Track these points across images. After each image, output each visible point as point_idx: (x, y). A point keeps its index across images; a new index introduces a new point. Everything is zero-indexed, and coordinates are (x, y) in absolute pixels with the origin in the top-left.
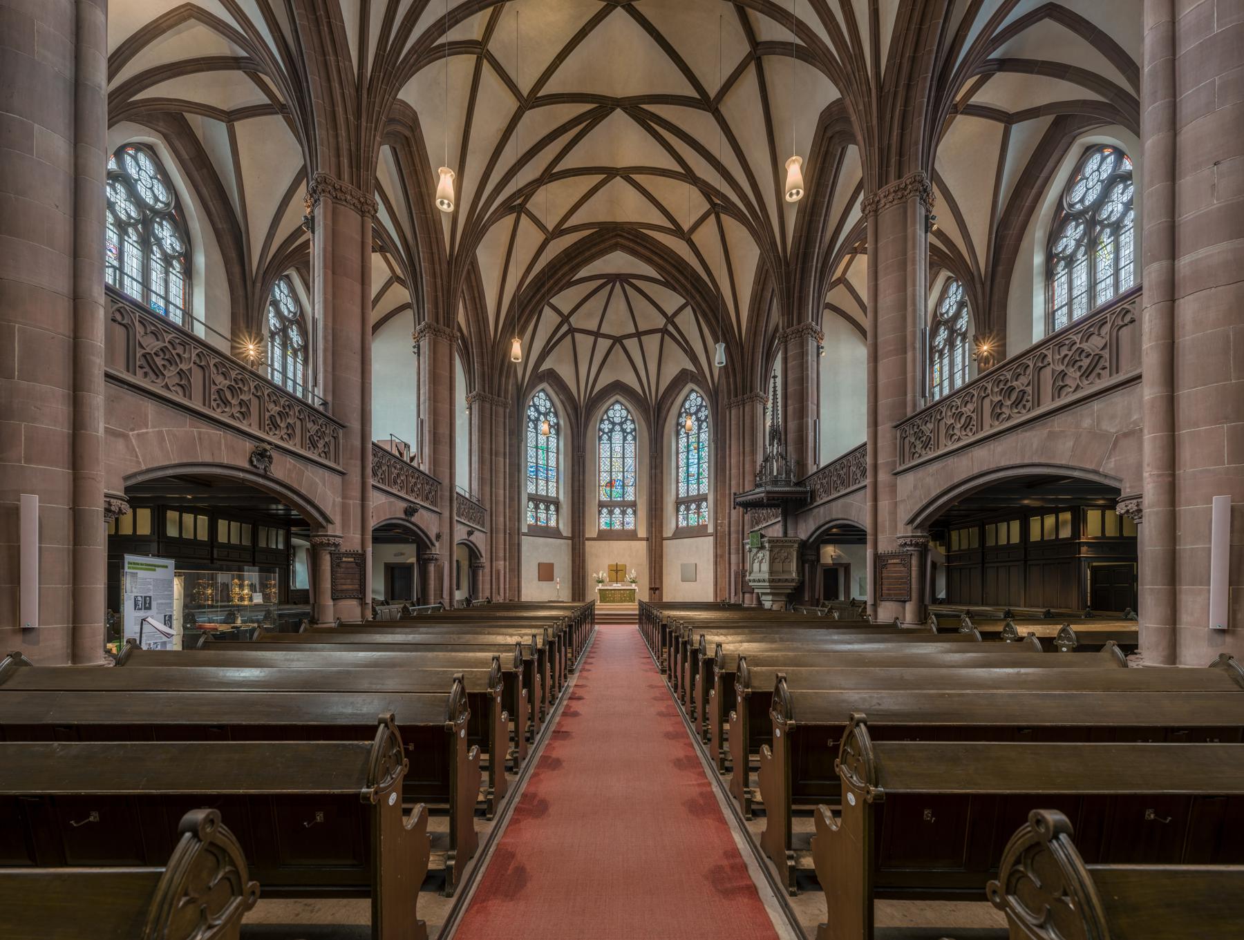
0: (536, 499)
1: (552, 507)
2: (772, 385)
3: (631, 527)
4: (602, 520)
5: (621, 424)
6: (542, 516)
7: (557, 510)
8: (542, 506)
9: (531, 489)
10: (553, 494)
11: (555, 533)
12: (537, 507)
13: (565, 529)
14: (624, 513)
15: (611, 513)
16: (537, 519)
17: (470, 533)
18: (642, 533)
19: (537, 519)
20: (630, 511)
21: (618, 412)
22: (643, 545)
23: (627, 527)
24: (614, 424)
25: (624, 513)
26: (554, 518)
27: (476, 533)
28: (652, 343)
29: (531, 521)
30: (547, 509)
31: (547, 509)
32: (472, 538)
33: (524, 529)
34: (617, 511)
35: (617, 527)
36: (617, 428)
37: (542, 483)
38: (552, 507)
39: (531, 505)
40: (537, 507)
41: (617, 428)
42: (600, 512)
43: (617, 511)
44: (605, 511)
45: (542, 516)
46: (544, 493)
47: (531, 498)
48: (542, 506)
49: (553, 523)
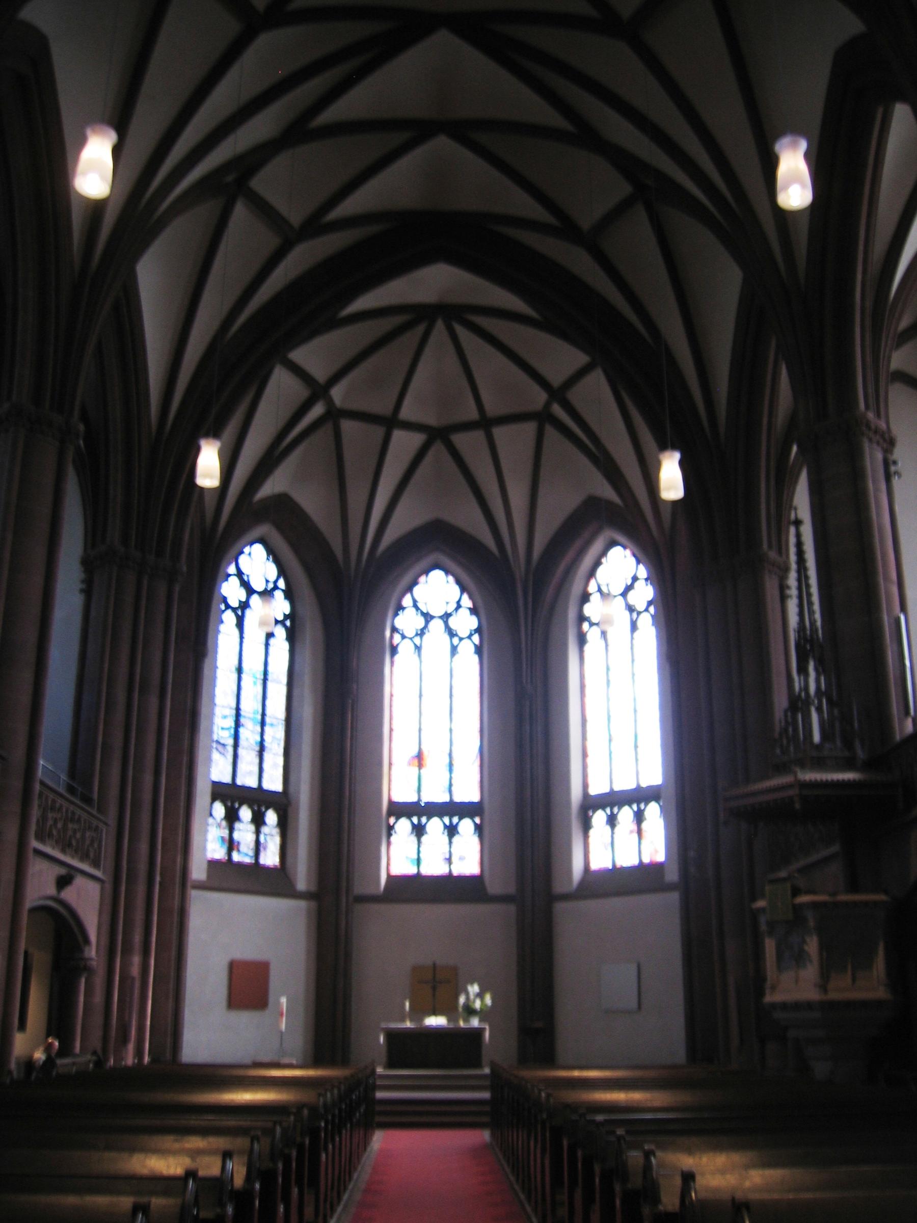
0: (231, 796)
1: (271, 817)
2: (792, 540)
5: (446, 617)
7: (283, 825)
8: (246, 813)
9: (219, 769)
10: (274, 782)
12: (232, 817)
16: (232, 845)
17: (63, 882)
19: (232, 845)
21: (437, 589)
24: (428, 617)
27: (79, 881)
28: (515, 441)
29: (215, 850)
30: (258, 821)
31: (258, 821)
32: (68, 894)
33: (198, 872)
36: (437, 626)
37: (248, 759)
38: (271, 817)
39: (219, 810)
40: (232, 817)
41: (437, 626)
46: (252, 783)
48: (246, 813)
49: (271, 858)
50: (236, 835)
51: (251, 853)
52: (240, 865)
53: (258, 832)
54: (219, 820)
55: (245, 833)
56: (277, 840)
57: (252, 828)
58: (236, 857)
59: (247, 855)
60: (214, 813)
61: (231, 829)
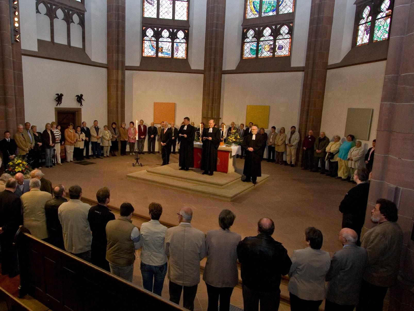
0: (158, 25)
1: (181, 34)
3: (285, 52)
4: (247, 47)
6: (166, 45)
7: (187, 37)
8: (165, 33)
11: (181, 66)
12: (157, 35)
13: (197, 63)
14: (276, 34)
15: (259, 35)
16: (158, 49)
18: (299, 60)
19: (158, 49)
23: (279, 53)
25: (276, 34)
26: (182, 47)
30: (173, 36)
31: (173, 36)
34: (267, 31)
35: (266, 53)
38: (181, 34)
40: (157, 35)
44: (251, 33)
45: (166, 45)
46: (170, 17)
47: (147, 23)
48: (165, 33)
49: (181, 54)
50: (160, 44)
51: (170, 53)
52: (163, 58)
53: (173, 43)
54: (150, 37)
56: (184, 46)
57: (64, 24)
58: (160, 55)
60: (147, 34)
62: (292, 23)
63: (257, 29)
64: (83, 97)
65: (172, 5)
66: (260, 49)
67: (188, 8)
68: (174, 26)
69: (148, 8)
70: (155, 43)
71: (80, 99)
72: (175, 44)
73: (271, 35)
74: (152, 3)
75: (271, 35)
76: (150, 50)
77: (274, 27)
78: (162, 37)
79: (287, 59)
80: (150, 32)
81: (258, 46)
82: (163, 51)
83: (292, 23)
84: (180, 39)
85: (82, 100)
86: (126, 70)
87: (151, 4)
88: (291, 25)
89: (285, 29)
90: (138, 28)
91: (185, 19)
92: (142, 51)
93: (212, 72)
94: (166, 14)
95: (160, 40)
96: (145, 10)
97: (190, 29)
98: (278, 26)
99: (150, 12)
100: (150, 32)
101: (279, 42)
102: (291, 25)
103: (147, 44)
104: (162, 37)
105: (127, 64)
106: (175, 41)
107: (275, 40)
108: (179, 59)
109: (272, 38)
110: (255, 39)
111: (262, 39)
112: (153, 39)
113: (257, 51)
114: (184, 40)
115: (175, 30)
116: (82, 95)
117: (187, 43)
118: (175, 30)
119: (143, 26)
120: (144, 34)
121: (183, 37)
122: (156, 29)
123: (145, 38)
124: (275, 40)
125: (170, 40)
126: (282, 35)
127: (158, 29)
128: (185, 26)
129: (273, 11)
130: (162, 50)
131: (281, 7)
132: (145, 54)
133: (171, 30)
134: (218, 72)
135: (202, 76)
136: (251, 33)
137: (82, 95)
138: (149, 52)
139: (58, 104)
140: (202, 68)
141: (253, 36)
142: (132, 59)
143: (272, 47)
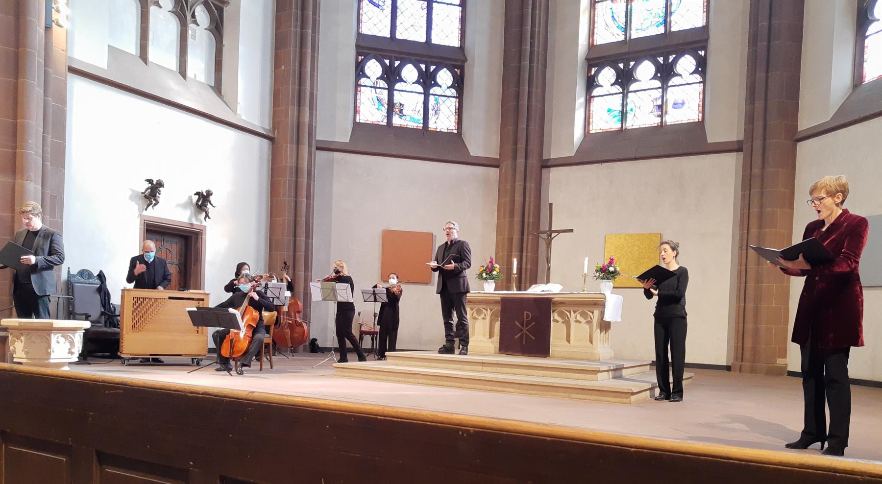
0: (391, 53)
1: (445, 77)
7: (459, 84)
8: (410, 72)
10: (446, 34)
11: (446, 148)
12: (391, 76)
13: (482, 140)
14: (665, 73)
15: (625, 79)
18: (727, 127)
20: (686, 64)
22: (729, 165)
25: (665, 73)
30: (427, 81)
31: (427, 81)
34: (645, 70)
35: (642, 116)
38: (445, 77)
40: (391, 76)
42: (591, 83)
43: (645, 70)
47: (367, 48)
48: (410, 72)
49: (444, 120)
50: (398, 98)
51: (420, 117)
52: (403, 130)
53: (426, 95)
54: (374, 78)
55: (409, 95)
56: (453, 103)
58: (397, 121)
59: (413, 119)
60: (367, 71)
61: (391, 91)
62: (705, 48)
63: (621, 66)
64: (212, 198)
65: (425, 11)
66: (631, 110)
67: (463, 20)
68: (429, 58)
69: (370, 14)
70: (386, 92)
71: (203, 201)
72: (432, 98)
73: (655, 77)
74: (381, 3)
75: (655, 77)
76: (374, 109)
77: (661, 60)
78: (401, 80)
79: (697, 128)
80: (374, 68)
81: (624, 105)
82: (404, 112)
83: (705, 48)
84: (444, 87)
85: (209, 206)
86: (318, 148)
87: (378, 6)
88: (702, 53)
89: (686, 64)
90: (349, 56)
91: (456, 43)
92: (356, 111)
93: (521, 161)
94: (411, 30)
95: (398, 86)
96: (364, 18)
97: (467, 66)
98: (671, 58)
99: (375, 24)
100: (374, 68)
101: (673, 95)
102: (702, 53)
103: (367, 96)
104: (401, 80)
105: (321, 135)
106: (431, 91)
107: (664, 88)
108: (440, 132)
109: (658, 84)
110: (618, 89)
111: (633, 87)
112: (382, 84)
113: (623, 115)
114: (453, 91)
115: (432, 68)
116: (209, 193)
117: (460, 97)
118: (432, 68)
119: (358, 54)
120: (360, 72)
121: (450, 83)
122: (387, 62)
123: (363, 81)
124: (664, 88)
125: (420, 89)
126: (680, 75)
127: (392, 63)
128: (455, 60)
129: (657, 26)
130: (401, 111)
131: (674, 18)
132: (361, 118)
133: (423, 66)
134: (533, 161)
135: (494, 172)
136: (607, 76)
137: (209, 193)
138: (371, 112)
139: (148, 206)
140: (493, 153)
141: (613, 80)
142: (333, 126)
143: (659, 103)
